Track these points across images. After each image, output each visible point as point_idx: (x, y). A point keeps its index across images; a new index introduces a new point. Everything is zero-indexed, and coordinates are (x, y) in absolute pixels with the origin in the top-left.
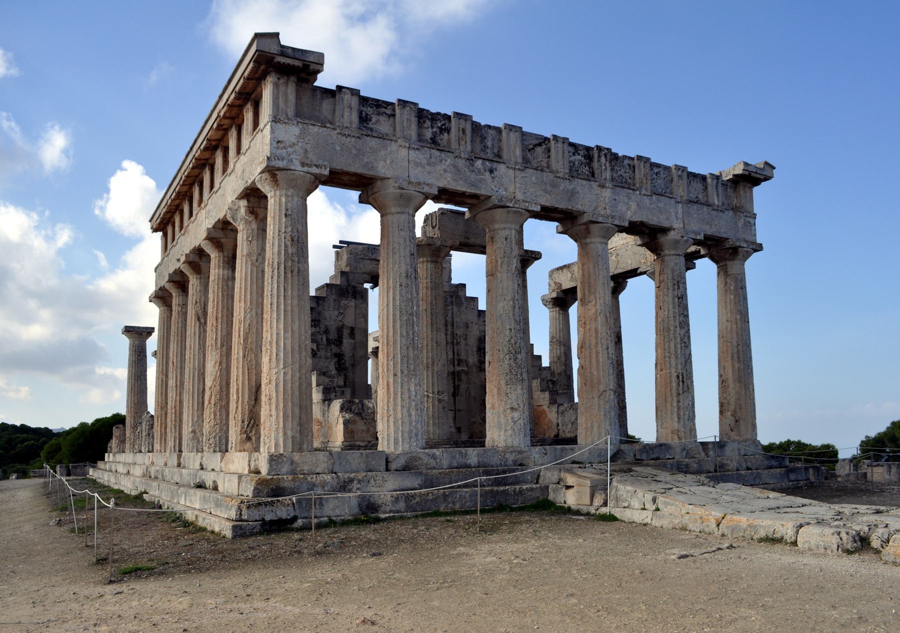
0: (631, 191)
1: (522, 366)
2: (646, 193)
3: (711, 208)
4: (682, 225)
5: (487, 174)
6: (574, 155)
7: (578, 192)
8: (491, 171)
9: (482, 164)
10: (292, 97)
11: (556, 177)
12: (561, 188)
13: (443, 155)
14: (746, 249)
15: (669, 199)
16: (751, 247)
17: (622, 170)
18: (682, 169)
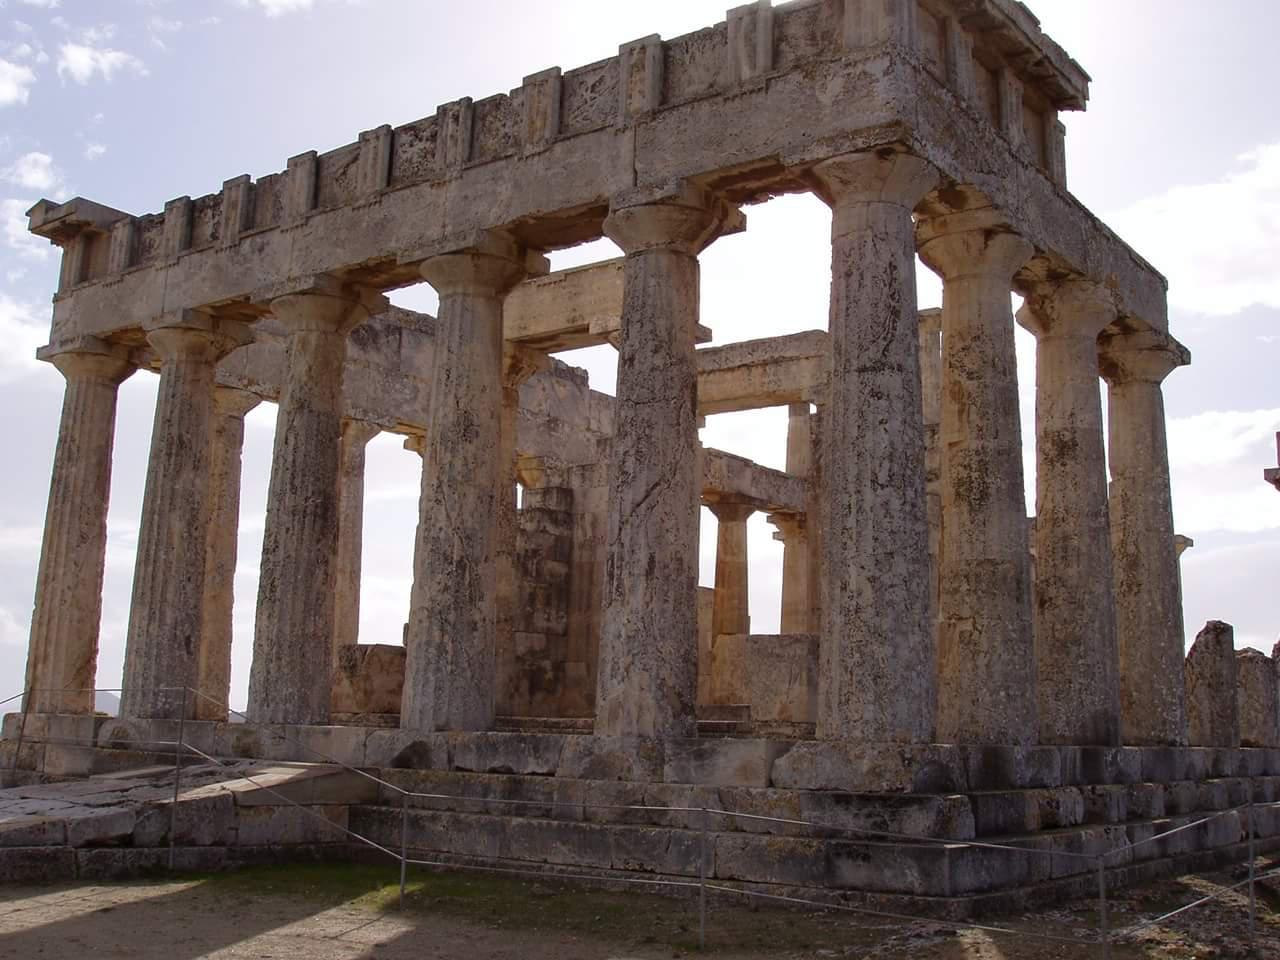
0: (503, 163)
1: (277, 575)
2: (537, 150)
3: (720, 99)
4: (628, 178)
5: (256, 257)
6: (411, 146)
7: (394, 218)
8: (261, 250)
9: (251, 245)
10: (76, 263)
11: (353, 209)
12: (364, 225)
13: (204, 256)
14: (830, 161)
15: (596, 134)
16: (847, 146)
17: (509, 124)
18: (639, 46)
